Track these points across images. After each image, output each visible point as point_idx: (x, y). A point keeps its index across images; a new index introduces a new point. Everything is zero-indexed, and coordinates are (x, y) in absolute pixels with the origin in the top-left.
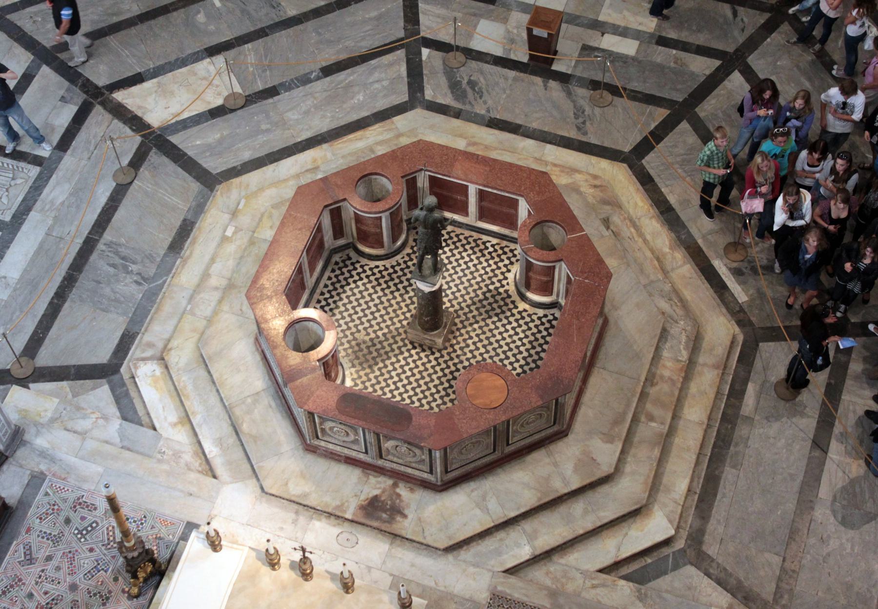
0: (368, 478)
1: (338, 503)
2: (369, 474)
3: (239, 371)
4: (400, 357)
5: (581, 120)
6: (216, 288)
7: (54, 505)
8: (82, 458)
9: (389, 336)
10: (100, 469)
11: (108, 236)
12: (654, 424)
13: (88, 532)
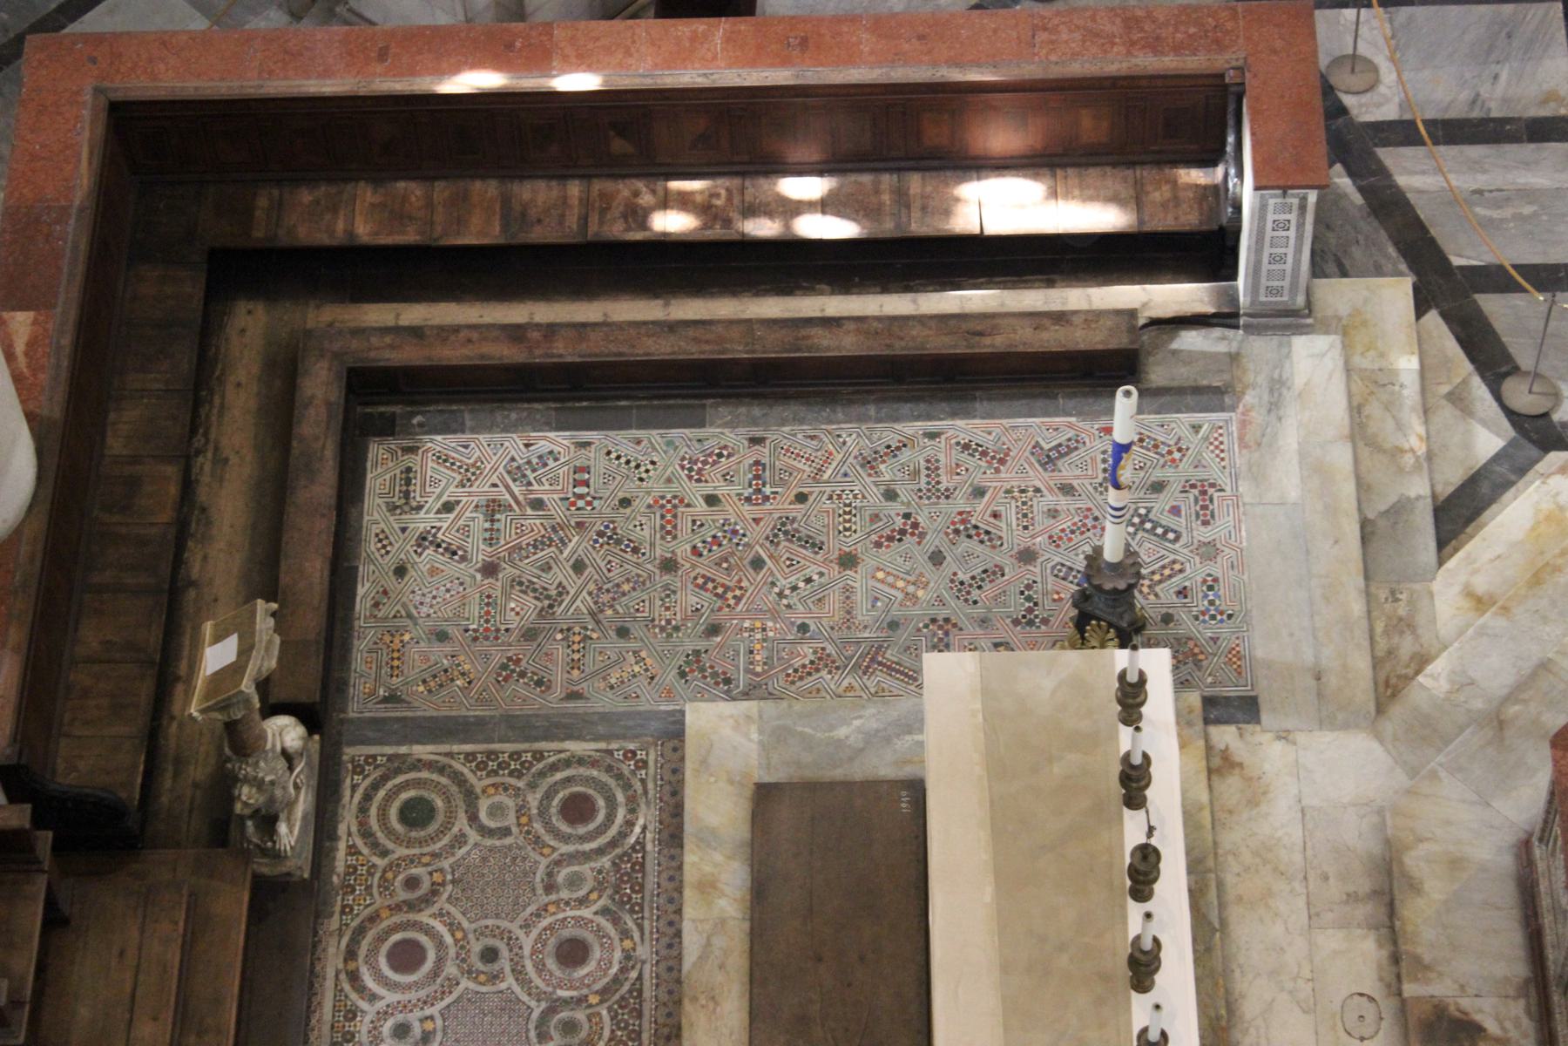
0: (1515, 998)
1: (1427, 958)
2: (1527, 996)
7: (1180, 450)
8: (1302, 455)
10: (1293, 494)
13: (1152, 531)
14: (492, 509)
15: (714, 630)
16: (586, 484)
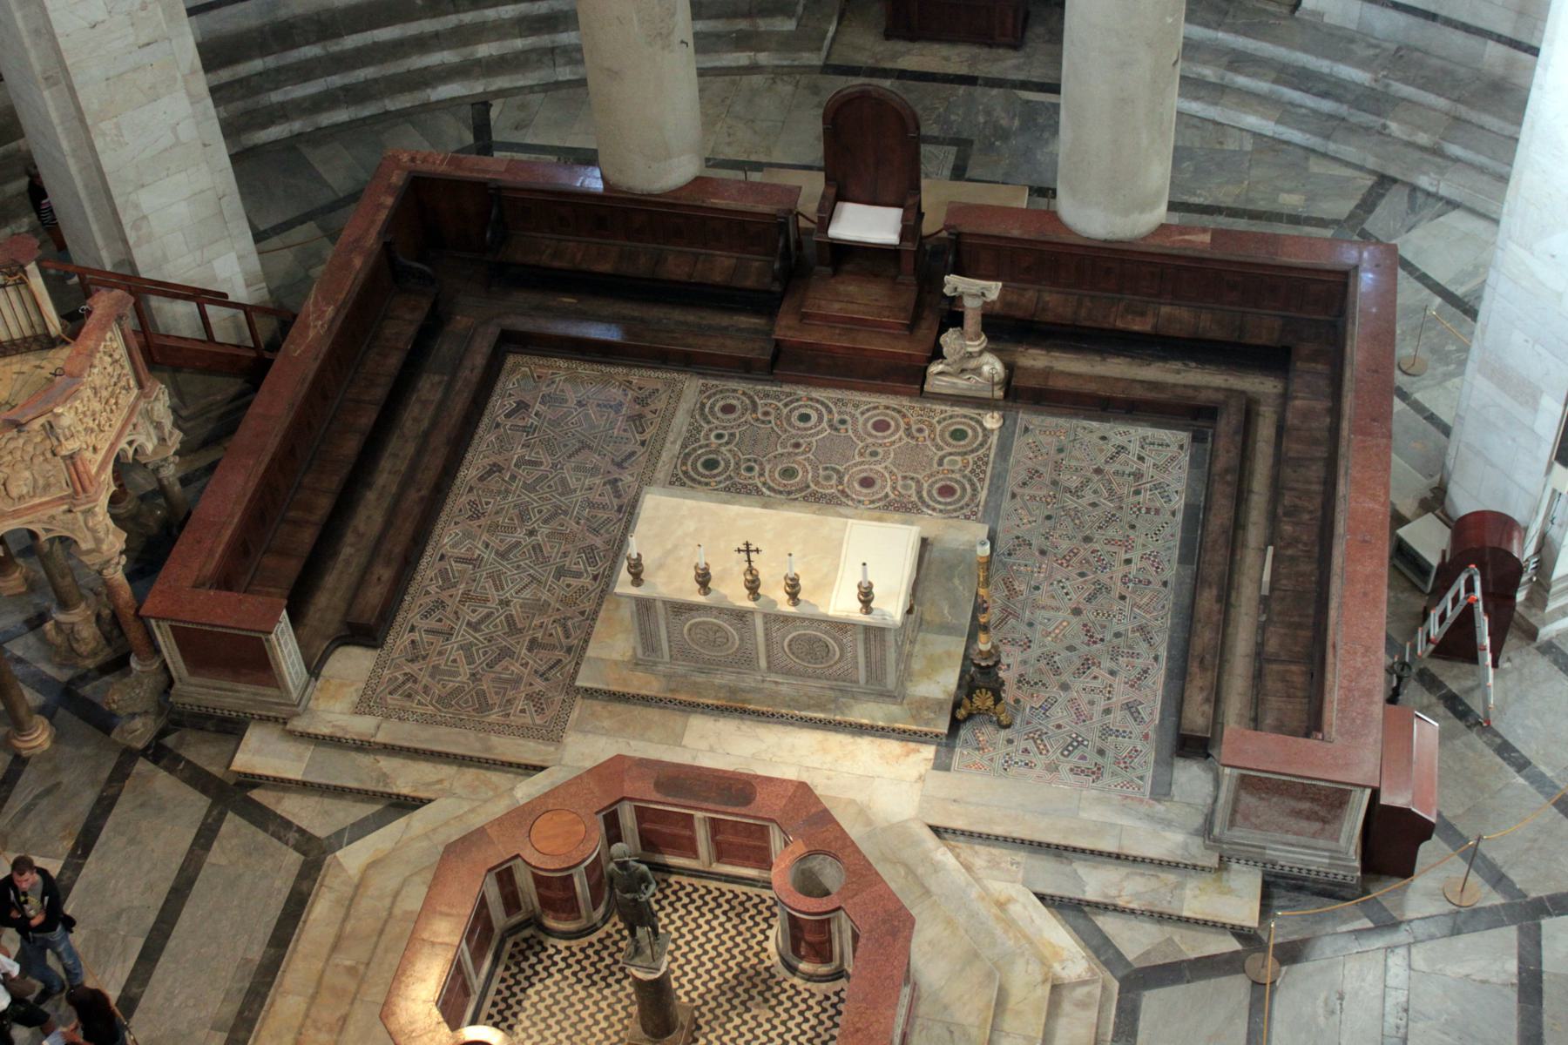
3: (930, 943)
4: (702, 989)
8: (1112, 825)
9: (724, 1019)
10: (1083, 815)
12: (348, 963)
14: (1138, 475)
15: (1043, 553)
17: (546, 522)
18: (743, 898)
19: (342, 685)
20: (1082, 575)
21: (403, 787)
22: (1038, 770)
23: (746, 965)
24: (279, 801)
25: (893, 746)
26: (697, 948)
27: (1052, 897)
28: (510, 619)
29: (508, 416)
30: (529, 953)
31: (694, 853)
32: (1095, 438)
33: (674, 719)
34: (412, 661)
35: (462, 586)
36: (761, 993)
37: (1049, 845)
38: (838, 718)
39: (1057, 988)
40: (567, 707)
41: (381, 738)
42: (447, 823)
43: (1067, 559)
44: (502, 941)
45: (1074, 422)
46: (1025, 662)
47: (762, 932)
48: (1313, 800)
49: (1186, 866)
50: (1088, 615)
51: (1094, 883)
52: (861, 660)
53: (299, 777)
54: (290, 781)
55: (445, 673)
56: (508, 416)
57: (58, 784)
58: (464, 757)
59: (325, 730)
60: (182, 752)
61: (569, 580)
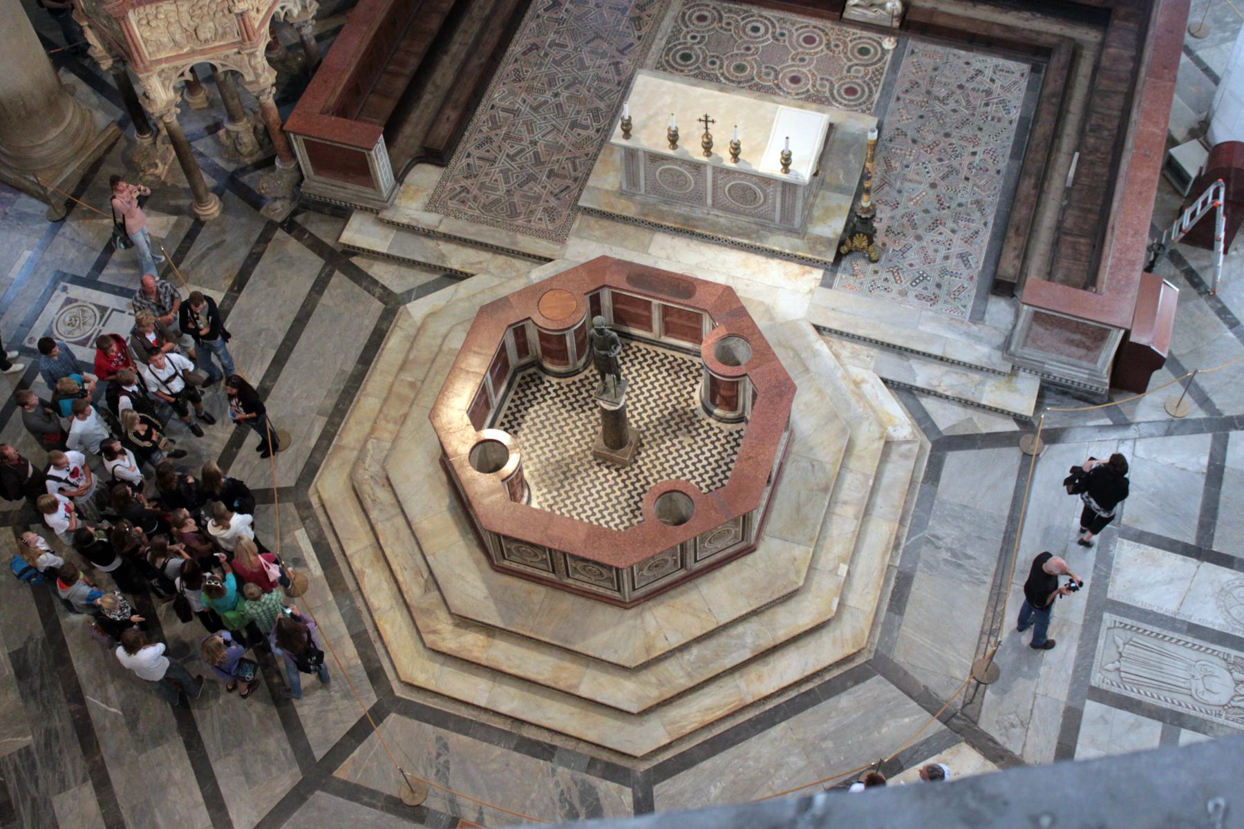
3: (805, 404)
4: (647, 420)
5: (442, 760)
6: (845, 503)
8: (941, 337)
9: (660, 441)
10: (921, 328)
11: (984, 592)
12: (410, 379)
14: (988, 93)
15: (914, 141)
16: (993, 119)
17: (567, 88)
18: (680, 361)
19: (417, 191)
20: (940, 160)
21: (455, 264)
22: (894, 294)
23: (678, 407)
24: (370, 266)
25: (794, 268)
26: (645, 392)
27: (893, 382)
28: (536, 154)
29: (546, 10)
30: (532, 384)
31: (650, 329)
32: (961, 63)
33: (644, 235)
34: (466, 178)
35: (505, 130)
36: (686, 427)
37: (894, 346)
38: (758, 244)
39: (888, 444)
40: (570, 219)
41: (442, 229)
42: (483, 291)
43: (930, 148)
44: (514, 375)
45: (948, 50)
46: (892, 218)
47: (691, 385)
48: (1082, 333)
49: (988, 370)
50: (942, 188)
51: (923, 375)
52: (778, 205)
53: (385, 251)
54: (378, 253)
55: (488, 188)
56: (546, 10)
57: (223, 241)
58: (497, 248)
59: (404, 220)
60: (307, 227)
61: (580, 131)
